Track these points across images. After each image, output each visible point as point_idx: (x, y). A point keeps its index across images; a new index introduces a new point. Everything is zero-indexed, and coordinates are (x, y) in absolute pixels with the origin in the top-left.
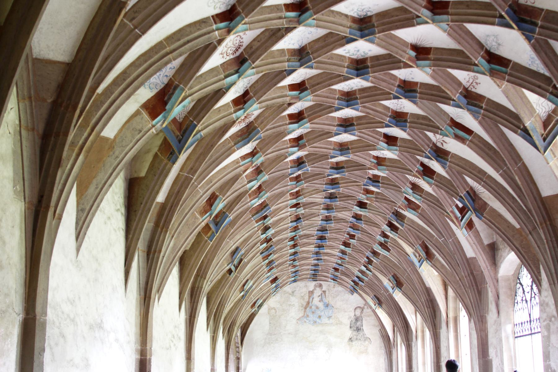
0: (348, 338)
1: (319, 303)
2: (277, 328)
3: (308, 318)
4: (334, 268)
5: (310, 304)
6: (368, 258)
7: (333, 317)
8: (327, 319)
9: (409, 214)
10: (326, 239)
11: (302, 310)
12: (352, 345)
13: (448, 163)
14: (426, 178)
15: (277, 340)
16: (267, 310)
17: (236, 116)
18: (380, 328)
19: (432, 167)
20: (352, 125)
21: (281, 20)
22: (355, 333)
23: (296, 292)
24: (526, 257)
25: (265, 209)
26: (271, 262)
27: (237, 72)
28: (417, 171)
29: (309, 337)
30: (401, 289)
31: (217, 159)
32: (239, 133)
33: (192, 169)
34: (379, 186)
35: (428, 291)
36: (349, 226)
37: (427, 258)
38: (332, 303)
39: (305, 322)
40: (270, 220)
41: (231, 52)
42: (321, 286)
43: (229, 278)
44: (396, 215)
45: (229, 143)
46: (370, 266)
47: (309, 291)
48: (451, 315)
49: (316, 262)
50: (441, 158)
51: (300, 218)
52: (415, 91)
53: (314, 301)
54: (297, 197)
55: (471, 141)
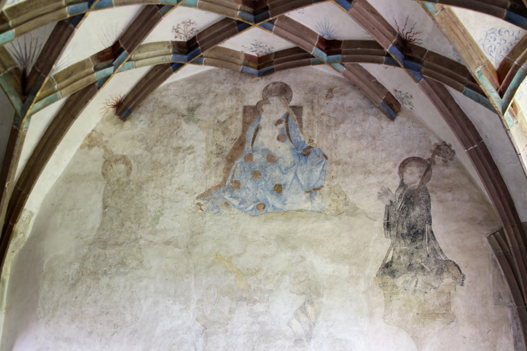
0: (380, 263)
1: (279, 144)
2: (128, 224)
3: (236, 192)
5: (248, 146)
7: (326, 189)
8: (304, 196)
11: (218, 164)
12: (394, 286)
15: (123, 263)
16: (100, 163)
18: (500, 223)
22: (403, 246)
23: (202, 109)
29: (239, 255)
39: (227, 204)
47: (246, 109)
53: (260, 139)
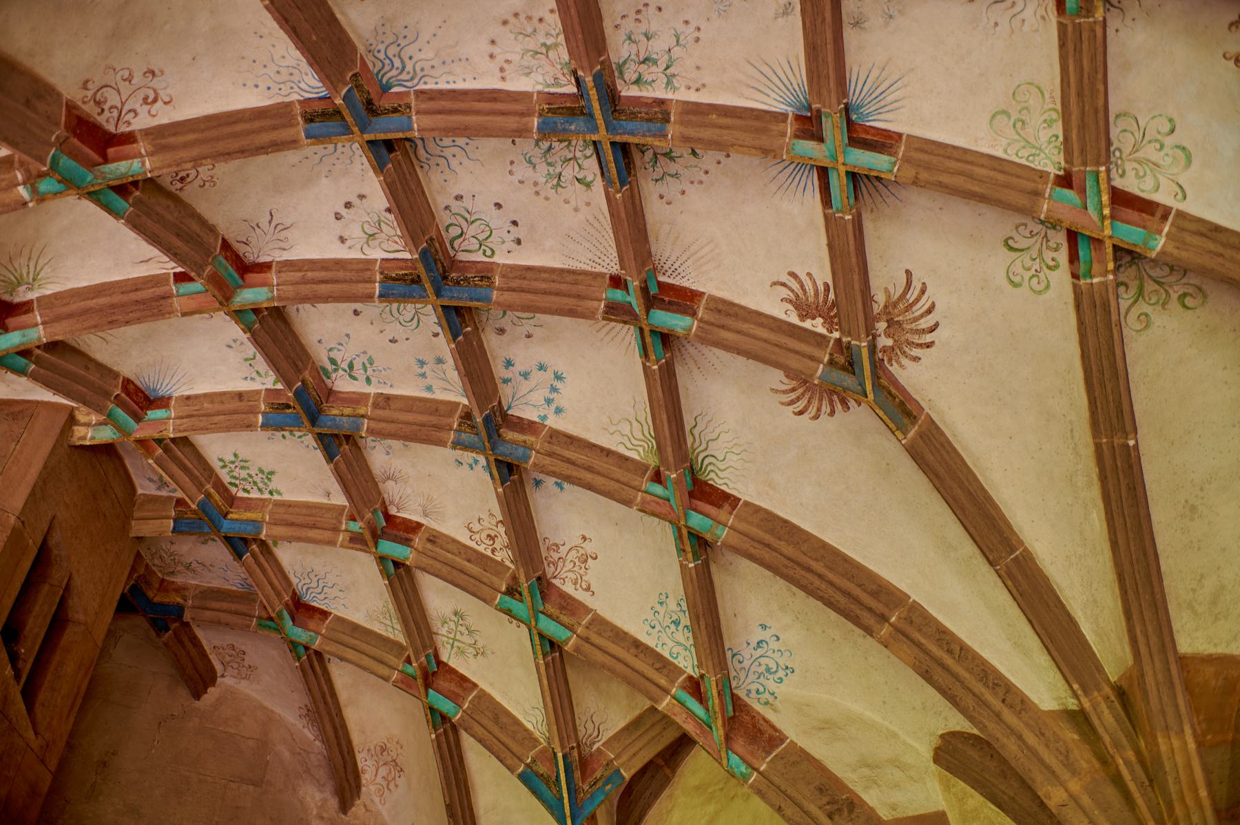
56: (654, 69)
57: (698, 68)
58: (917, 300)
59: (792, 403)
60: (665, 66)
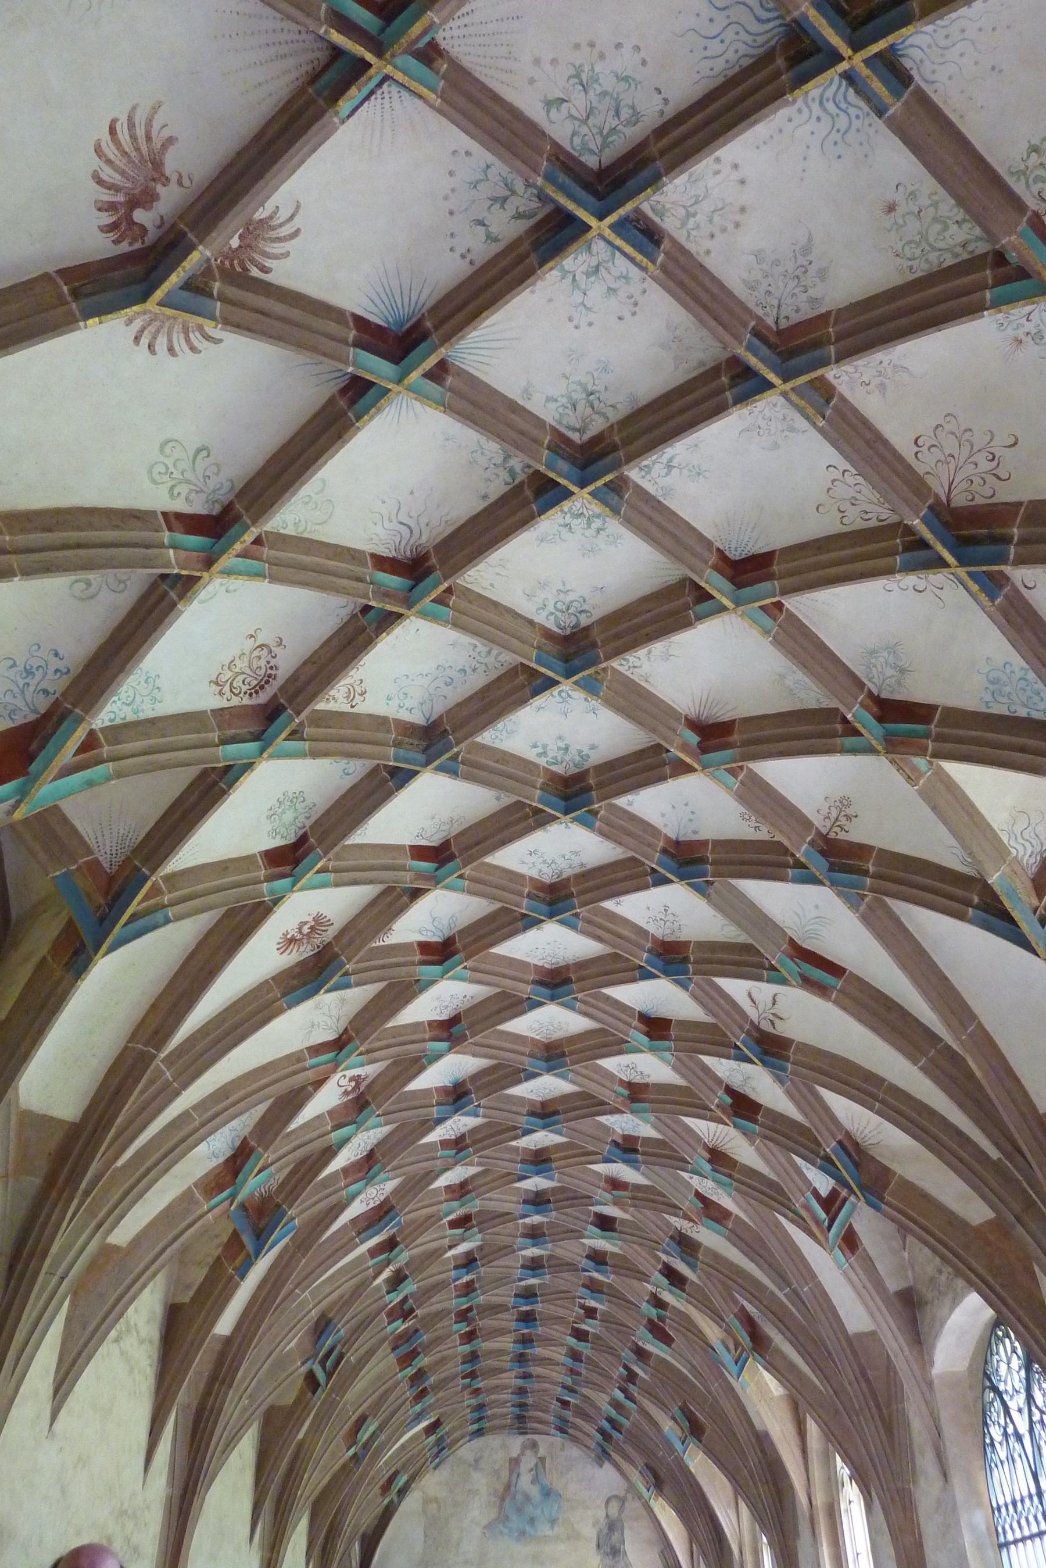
1: (532, 1486)
4: (558, 1400)
5: (513, 1489)
6: (626, 1367)
7: (561, 1520)
9: (707, 1236)
10: (535, 1320)
11: (494, 1503)
13: (789, 1066)
14: (738, 1120)
17: (272, 892)
19: (753, 1096)
20: (567, 981)
21: (361, 585)
24: (1010, 1301)
25: (387, 1219)
26: (419, 1376)
27: (256, 737)
28: (718, 1106)
30: (701, 1442)
31: (236, 1028)
32: (298, 970)
33: (156, 1032)
34: (636, 1161)
35: (763, 1441)
36: (581, 1282)
37: (754, 1349)
38: (558, 1485)
39: (501, 1533)
40: (402, 1251)
41: (244, 688)
42: (534, 1445)
43: (313, 1402)
44: (679, 1243)
45: (268, 992)
46: (632, 1388)
47: (511, 1460)
48: (819, 1499)
49: (520, 1382)
50: (773, 1055)
51: (475, 1260)
52: (703, 860)
53: (520, 1483)
54: (461, 1197)
55: (840, 991)
56: (584, 268)
57: (550, 300)
58: (188, 340)
59: (131, 125)
60: (577, 278)
